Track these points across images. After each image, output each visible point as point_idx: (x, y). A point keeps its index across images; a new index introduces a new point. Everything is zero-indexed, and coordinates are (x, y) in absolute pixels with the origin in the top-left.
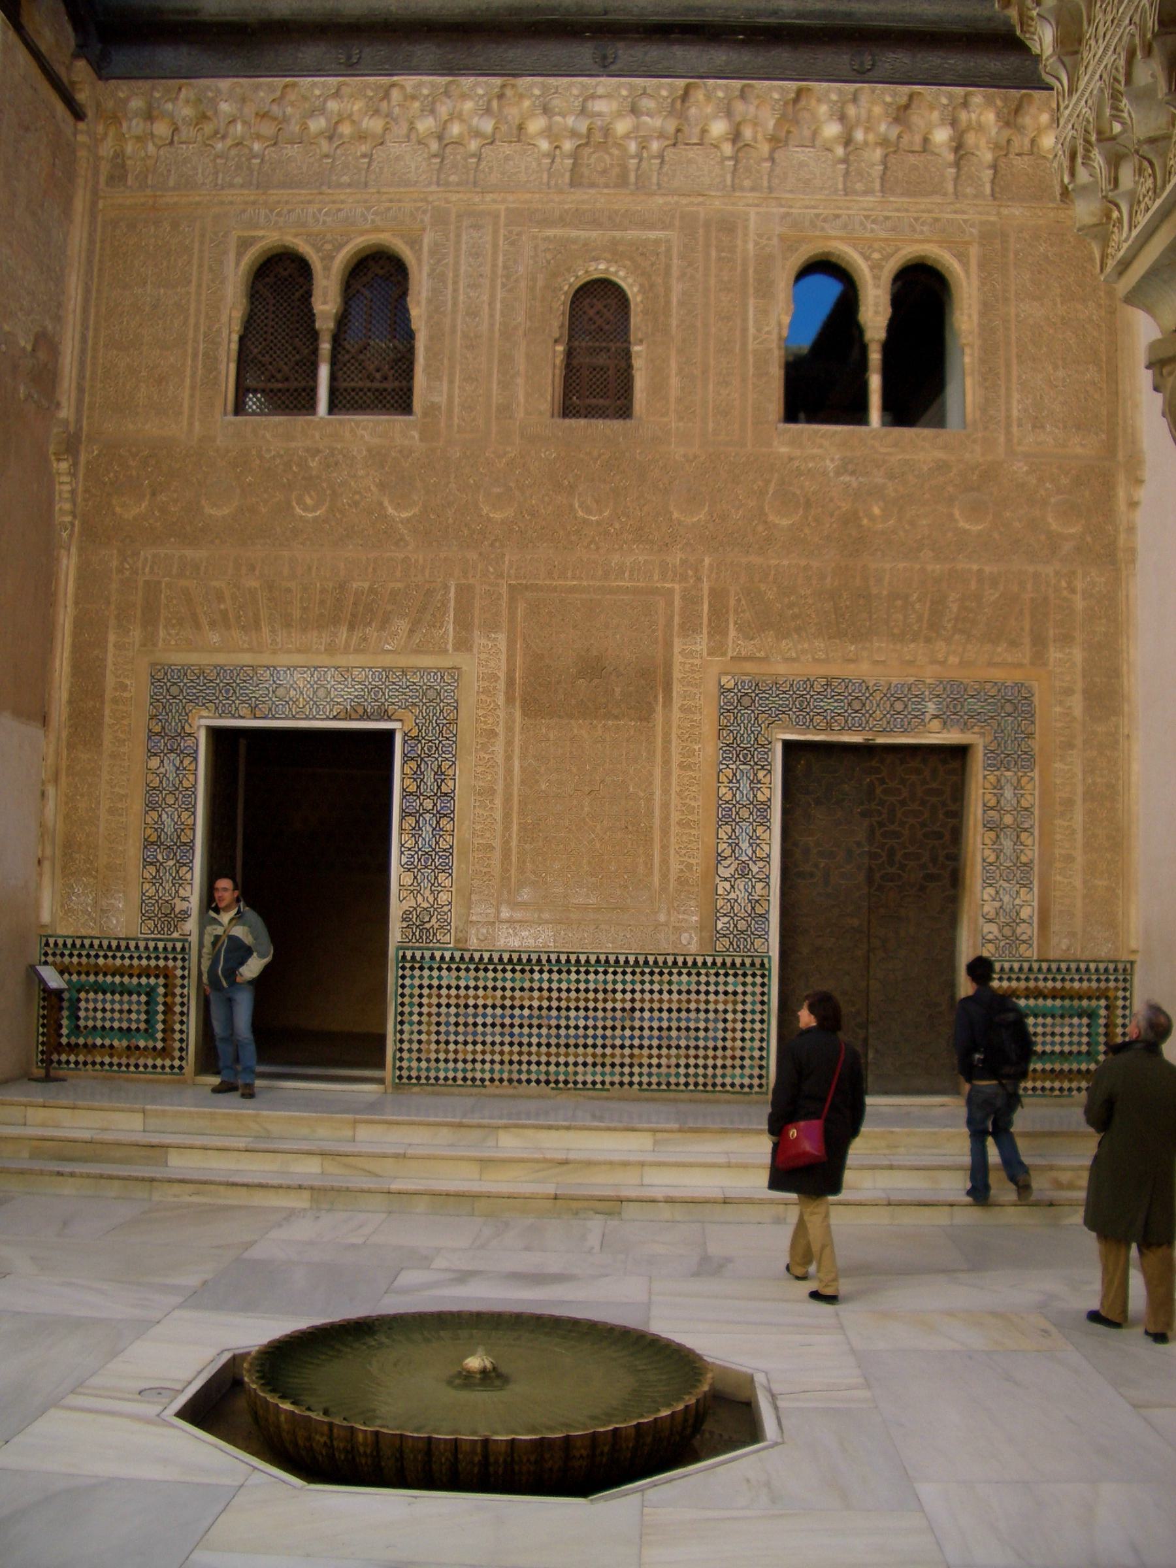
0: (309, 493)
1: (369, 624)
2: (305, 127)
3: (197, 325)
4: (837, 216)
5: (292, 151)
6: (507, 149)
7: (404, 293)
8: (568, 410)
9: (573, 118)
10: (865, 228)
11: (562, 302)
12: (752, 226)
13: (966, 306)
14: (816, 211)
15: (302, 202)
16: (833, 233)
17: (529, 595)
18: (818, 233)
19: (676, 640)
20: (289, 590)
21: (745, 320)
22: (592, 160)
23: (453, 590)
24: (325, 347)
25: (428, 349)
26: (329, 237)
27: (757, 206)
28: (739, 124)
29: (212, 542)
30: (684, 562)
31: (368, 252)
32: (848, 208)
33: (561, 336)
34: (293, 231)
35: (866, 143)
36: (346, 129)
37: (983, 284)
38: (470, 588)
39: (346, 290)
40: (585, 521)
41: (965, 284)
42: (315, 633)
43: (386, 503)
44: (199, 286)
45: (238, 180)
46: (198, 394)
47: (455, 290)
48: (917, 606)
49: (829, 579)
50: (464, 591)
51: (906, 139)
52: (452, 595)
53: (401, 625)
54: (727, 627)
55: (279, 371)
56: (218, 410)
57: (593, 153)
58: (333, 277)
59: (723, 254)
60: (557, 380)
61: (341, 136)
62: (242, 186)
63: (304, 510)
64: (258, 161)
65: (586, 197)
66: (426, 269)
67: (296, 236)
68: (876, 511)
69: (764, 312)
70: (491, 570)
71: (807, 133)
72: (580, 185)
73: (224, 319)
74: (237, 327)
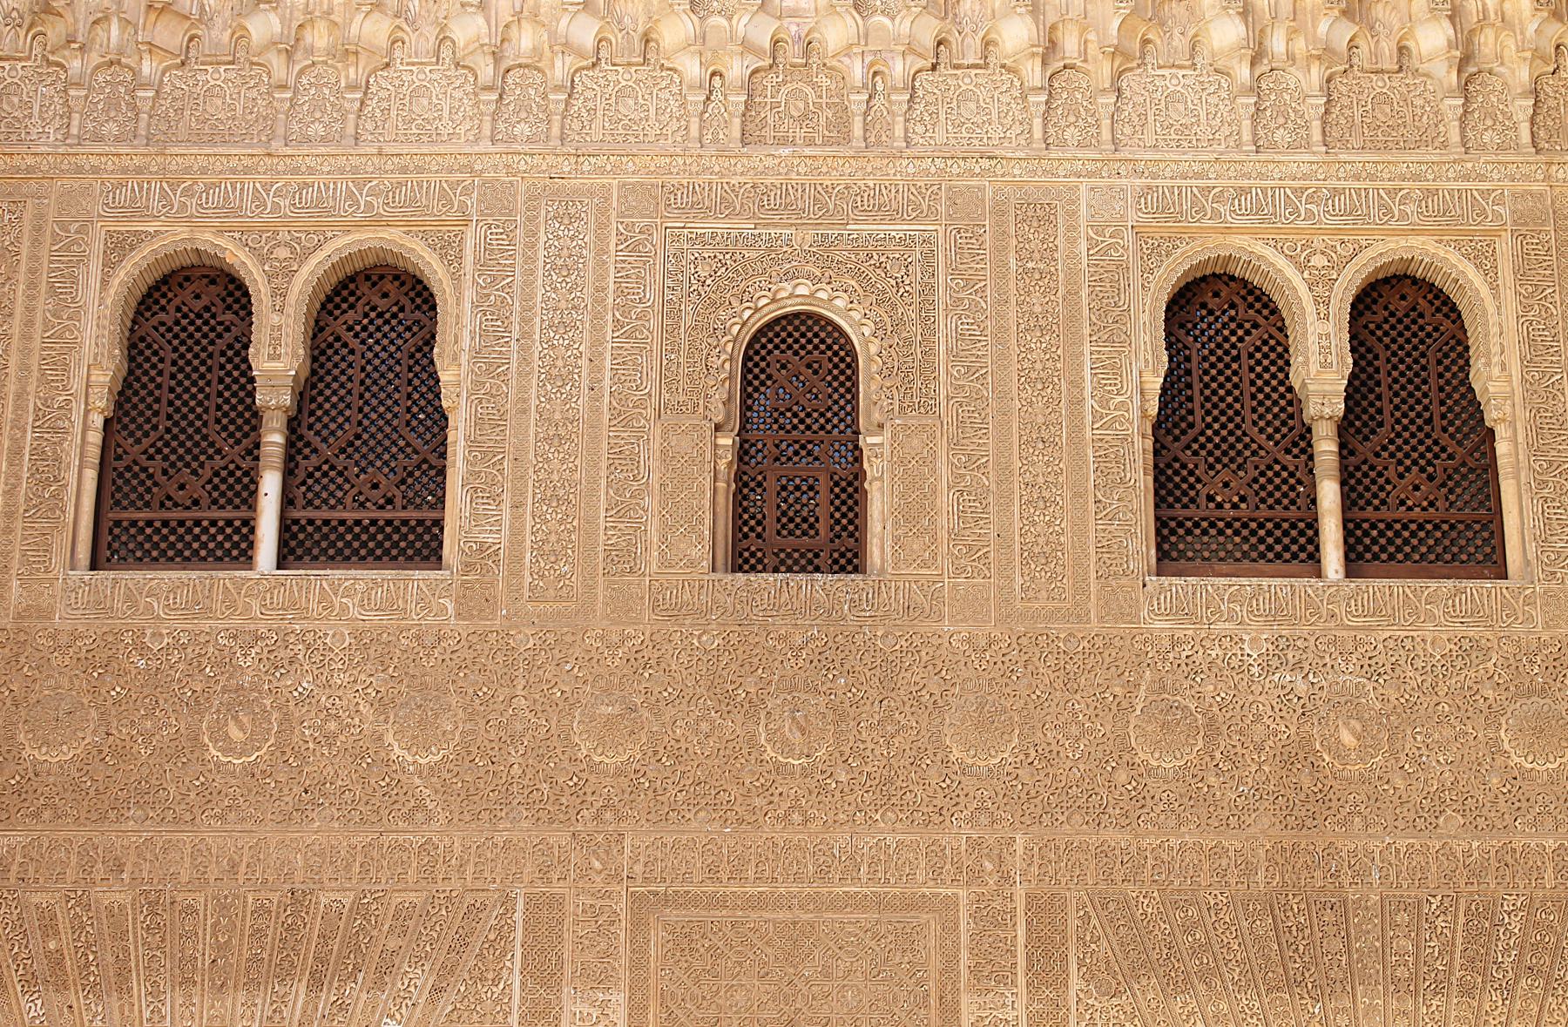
0: (235, 718)
1: (352, 977)
2: (240, 35)
3: (19, 396)
4: (1243, 191)
5: (214, 76)
6: (624, 77)
7: (430, 341)
8: (743, 560)
9: (745, 20)
10: (1296, 210)
11: (726, 360)
12: (1083, 208)
13: (1496, 349)
14: (1201, 183)
15: (234, 171)
16: (1237, 224)
17: (672, 914)
18: (1207, 223)
19: (965, 999)
20: (191, 911)
21: (1076, 384)
22: (781, 98)
23: (520, 905)
24: (274, 439)
25: (472, 443)
26: (283, 236)
27: (1090, 174)
28: (1053, 28)
29: (36, 815)
30: (975, 845)
31: (359, 266)
32: (1261, 176)
33: (728, 416)
34: (216, 222)
35: (1291, 57)
36: (319, 38)
37: (1527, 308)
38: (556, 902)
39: (315, 336)
40: (779, 768)
41: (1491, 309)
42: (241, 997)
43: (389, 738)
44: (29, 323)
45: (112, 128)
46: (19, 524)
47: (527, 335)
48: (1440, 922)
49: (1260, 876)
50: (545, 911)
51: (1364, 47)
52: (519, 916)
53: (421, 979)
54: (1065, 971)
55: (182, 487)
56: (58, 560)
57: (785, 82)
58: (290, 310)
59: (1030, 265)
60: (721, 499)
61: (310, 51)
62: (117, 139)
63: (224, 751)
64: (151, 94)
65: (769, 162)
66: (469, 294)
67: (220, 232)
68: (1347, 738)
69: (1110, 371)
70: (597, 865)
71: (1180, 43)
72: (761, 141)
73: (77, 385)
74: (102, 403)
